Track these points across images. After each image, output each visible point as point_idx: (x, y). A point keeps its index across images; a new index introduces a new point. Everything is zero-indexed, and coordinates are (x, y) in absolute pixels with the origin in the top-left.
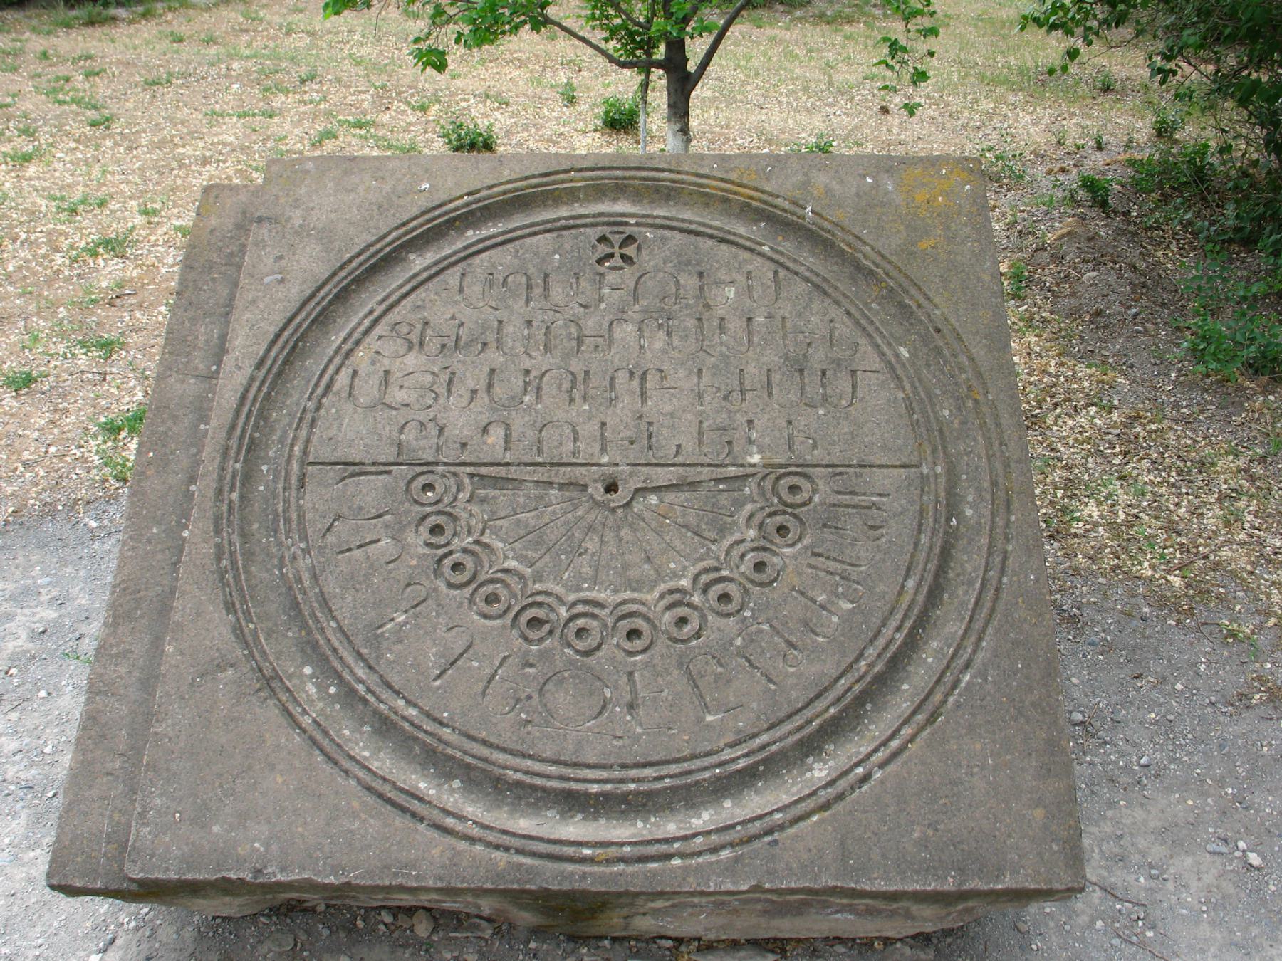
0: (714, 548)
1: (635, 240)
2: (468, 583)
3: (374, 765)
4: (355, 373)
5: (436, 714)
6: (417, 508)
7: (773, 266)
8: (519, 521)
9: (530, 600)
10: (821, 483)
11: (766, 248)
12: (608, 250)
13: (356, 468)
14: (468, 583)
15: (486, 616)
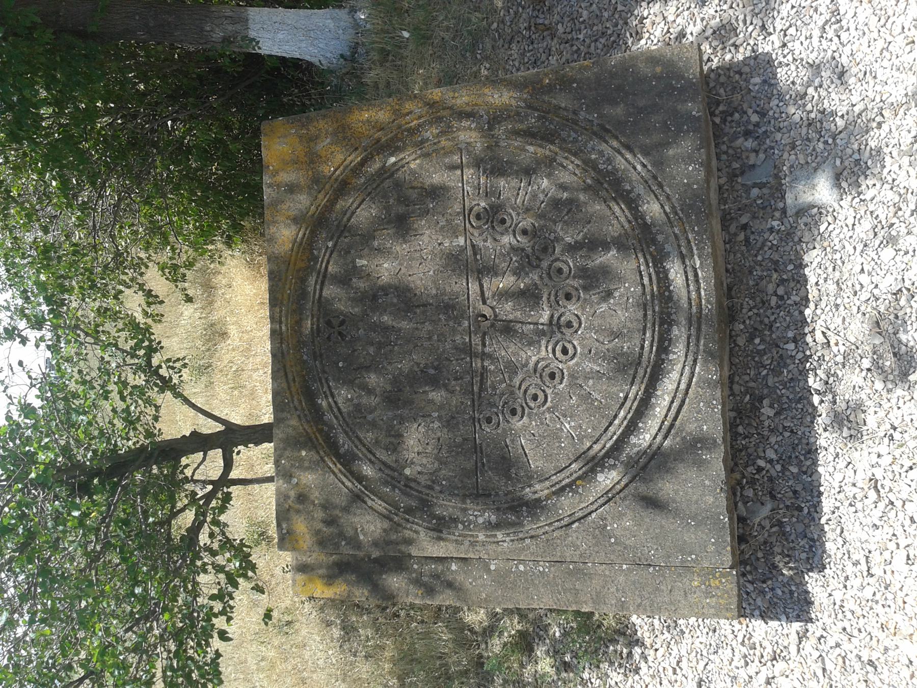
0: (514, 259)
1: (329, 320)
2: (544, 391)
3: (654, 432)
4: (419, 473)
5: (621, 401)
6: (501, 425)
7: (342, 239)
8: (505, 367)
9: (551, 355)
10: (474, 203)
11: (330, 244)
12: (336, 334)
13: (479, 464)
14: (544, 391)
15: (563, 378)
